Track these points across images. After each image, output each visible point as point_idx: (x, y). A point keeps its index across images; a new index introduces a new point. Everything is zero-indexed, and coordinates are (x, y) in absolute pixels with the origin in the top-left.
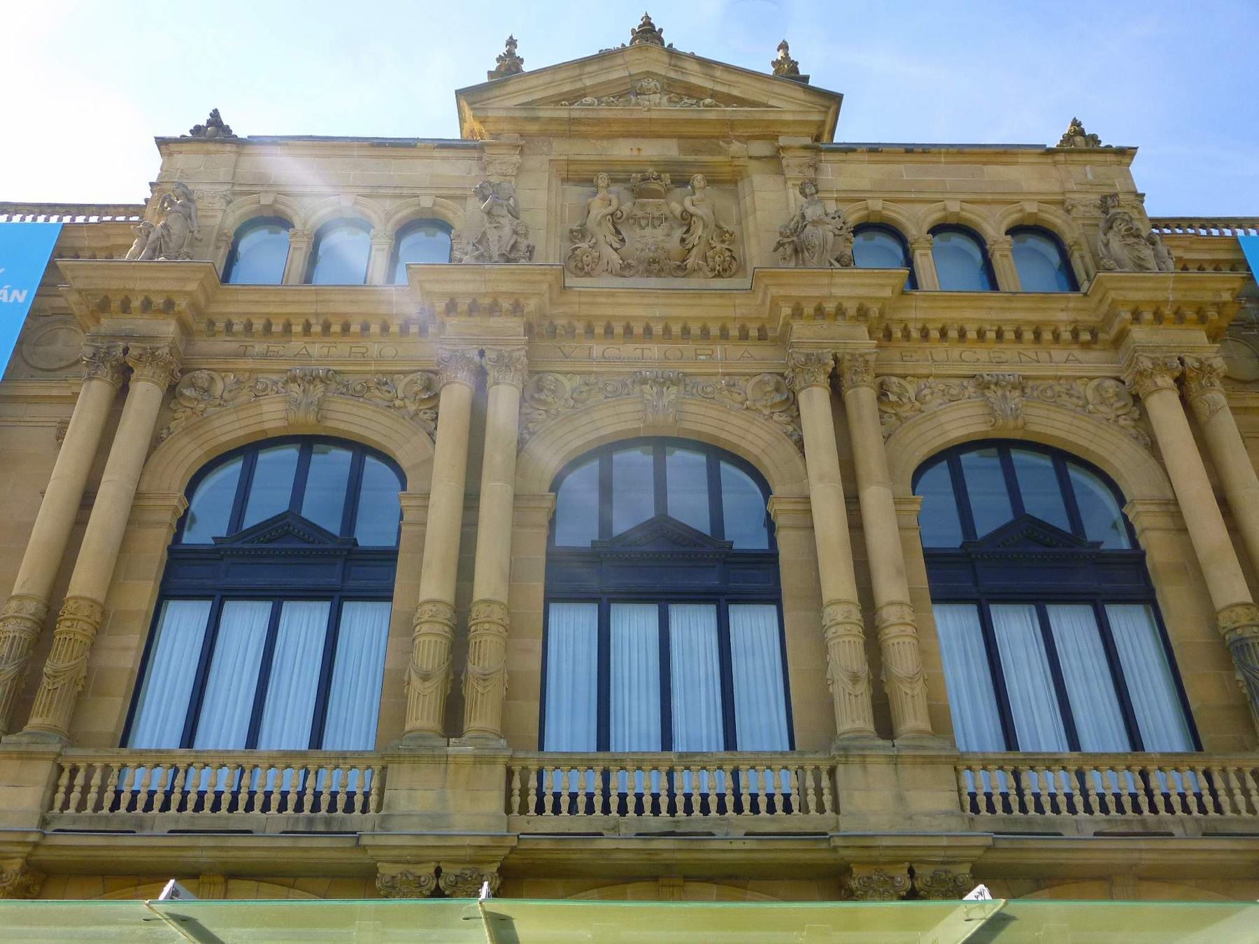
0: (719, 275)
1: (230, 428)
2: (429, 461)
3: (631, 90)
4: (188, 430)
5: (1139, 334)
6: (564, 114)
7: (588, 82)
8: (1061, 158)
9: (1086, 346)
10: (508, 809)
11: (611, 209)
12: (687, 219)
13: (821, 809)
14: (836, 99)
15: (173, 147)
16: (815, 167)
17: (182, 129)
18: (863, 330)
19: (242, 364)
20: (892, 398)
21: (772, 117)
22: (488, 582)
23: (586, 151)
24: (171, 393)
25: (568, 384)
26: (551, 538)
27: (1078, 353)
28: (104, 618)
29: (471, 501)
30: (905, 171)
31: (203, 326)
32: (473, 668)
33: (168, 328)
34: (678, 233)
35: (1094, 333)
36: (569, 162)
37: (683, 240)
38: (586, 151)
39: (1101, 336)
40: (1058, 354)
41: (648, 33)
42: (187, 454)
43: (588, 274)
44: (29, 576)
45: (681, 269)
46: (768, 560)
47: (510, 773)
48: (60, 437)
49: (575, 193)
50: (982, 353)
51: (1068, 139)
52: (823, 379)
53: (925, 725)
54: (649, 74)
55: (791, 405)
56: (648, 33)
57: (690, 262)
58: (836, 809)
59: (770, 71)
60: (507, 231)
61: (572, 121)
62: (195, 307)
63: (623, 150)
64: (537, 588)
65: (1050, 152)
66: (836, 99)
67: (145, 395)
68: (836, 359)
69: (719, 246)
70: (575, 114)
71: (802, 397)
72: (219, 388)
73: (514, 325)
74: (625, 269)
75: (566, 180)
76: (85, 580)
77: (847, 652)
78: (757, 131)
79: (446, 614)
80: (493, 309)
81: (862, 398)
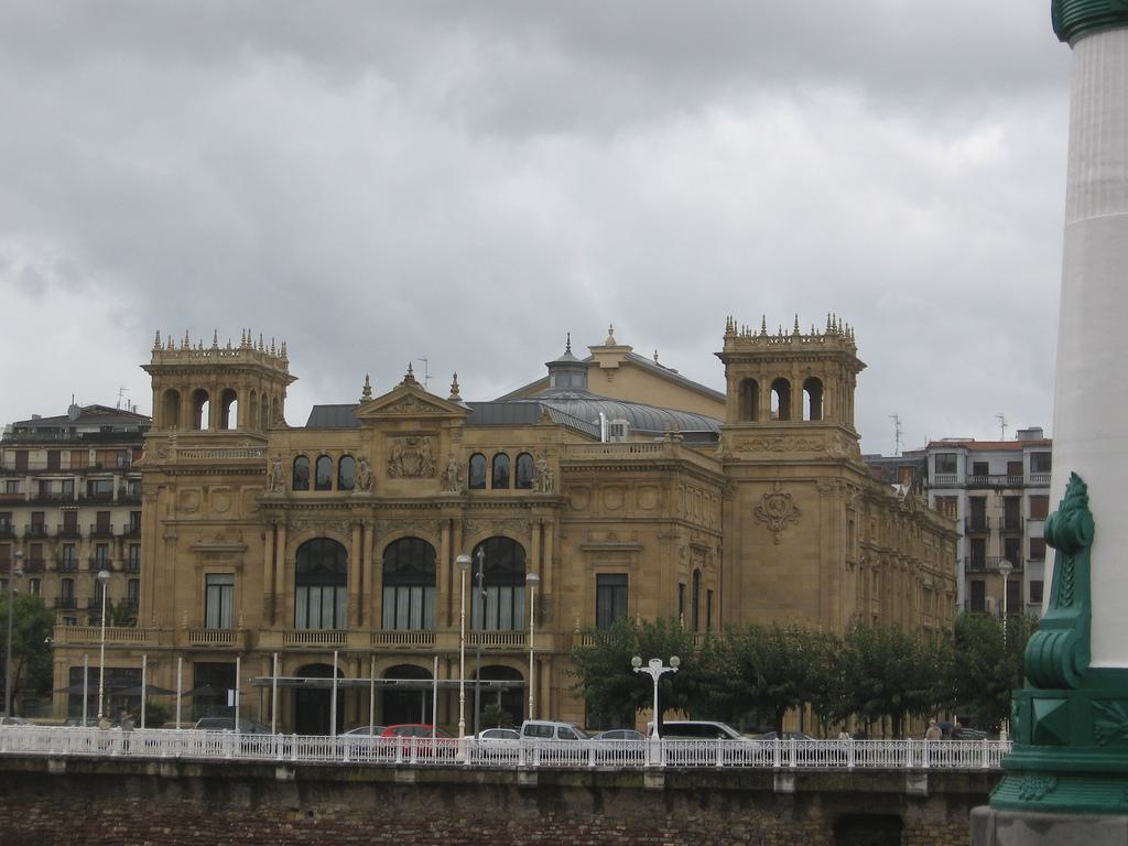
1: (303, 538)
4: (294, 539)
5: (535, 511)
12: (421, 456)
16: (461, 435)
22: (367, 590)
24: (287, 530)
25: (386, 523)
28: (285, 595)
29: (362, 560)
32: (364, 611)
40: (517, 511)
41: (409, 379)
42: (294, 546)
44: (267, 588)
48: (264, 538)
49: (390, 441)
52: (447, 527)
54: (410, 395)
56: (409, 379)
63: (404, 427)
64: (379, 586)
68: (451, 520)
74: (404, 476)
76: (279, 589)
79: (356, 597)
80: (363, 505)
81: (458, 533)
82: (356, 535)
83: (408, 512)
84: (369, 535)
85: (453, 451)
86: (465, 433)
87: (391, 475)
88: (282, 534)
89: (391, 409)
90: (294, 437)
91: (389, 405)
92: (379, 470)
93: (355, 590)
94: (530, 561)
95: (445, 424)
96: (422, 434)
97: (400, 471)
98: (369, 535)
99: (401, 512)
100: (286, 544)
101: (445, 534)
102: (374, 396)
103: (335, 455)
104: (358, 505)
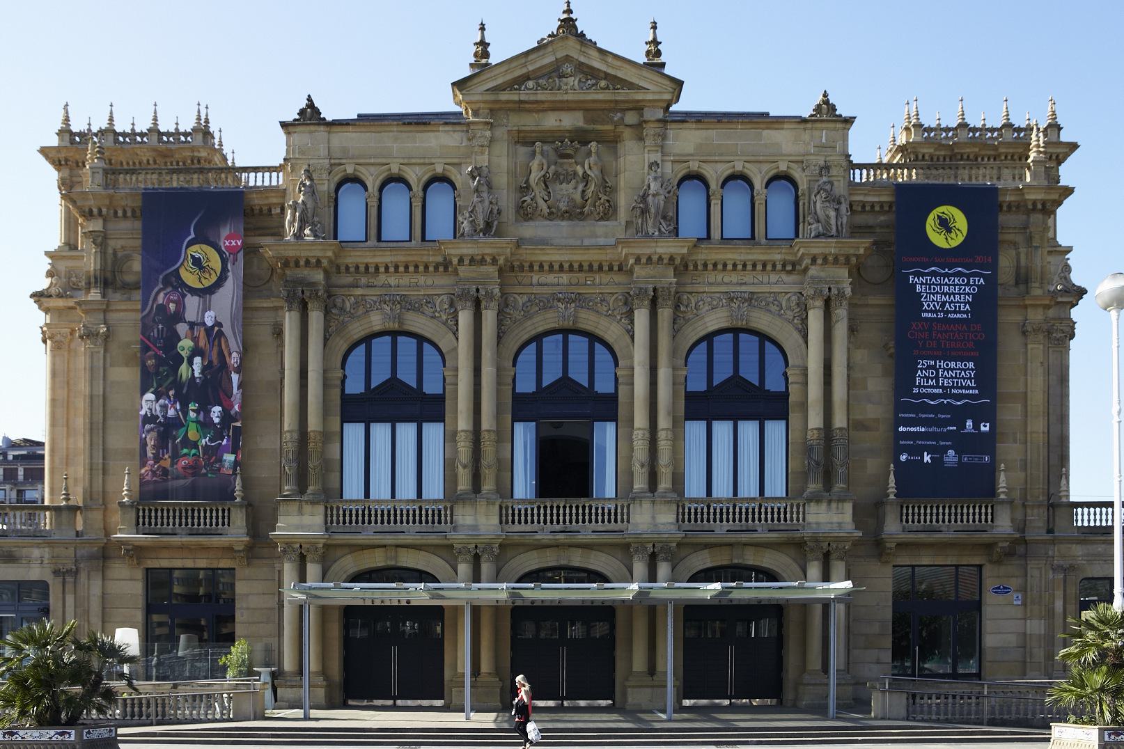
0: (601, 219)
2: (455, 349)
3: (555, 71)
6: (516, 98)
7: (531, 68)
8: (809, 125)
9: (789, 272)
10: (501, 522)
11: (543, 173)
13: (622, 521)
14: (680, 84)
15: (291, 129)
16: (664, 137)
17: (292, 115)
18: (671, 272)
19: (359, 291)
20: (683, 308)
21: (639, 96)
22: (487, 423)
23: (529, 122)
24: (327, 312)
26: (514, 389)
27: (785, 277)
30: (713, 135)
31: (334, 269)
32: (484, 462)
33: (319, 276)
34: (581, 187)
35: (794, 265)
36: (519, 132)
37: (584, 191)
38: (529, 122)
39: (798, 267)
41: (568, 24)
43: (531, 219)
45: (581, 216)
46: (613, 399)
47: (501, 508)
50: (734, 278)
51: (818, 109)
53: (669, 485)
55: (630, 315)
57: (586, 209)
58: (628, 521)
59: (641, 59)
60: (487, 203)
61: (521, 102)
62: (331, 262)
63: (551, 121)
65: (803, 121)
66: (680, 84)
67: (316, 319)
68: (655, 290)
69: (604, 198)
70: (523, 98)
71: (636, 312)
72: (348, 305)
73: (492, 270)
74: (551, 216)
75: (517, 142)
76: (314, 423)
77: (640, 451)
78: (631, 106)
80: (482, 262)
81: (665, 314)
82: (465, 318)
83: (564, 278)
84: (489, 317)
85: (635, 166)
86: (671, 133)
87: (525, 213)
88: (316, 319)
89: (531, 84)
90: (340, 139)
91: (527, 77)
92: (507, 200)
93: (464, 423)
94: (805, 371)
95: (631, 118)
96: (581, 138)
97: (543, 206)
98: (489, 317)
99: (551, 278)
100: (326, 340)
101: (641, 318)
102: (493, 60)
103: (415, 176)
104: (472, 261)
